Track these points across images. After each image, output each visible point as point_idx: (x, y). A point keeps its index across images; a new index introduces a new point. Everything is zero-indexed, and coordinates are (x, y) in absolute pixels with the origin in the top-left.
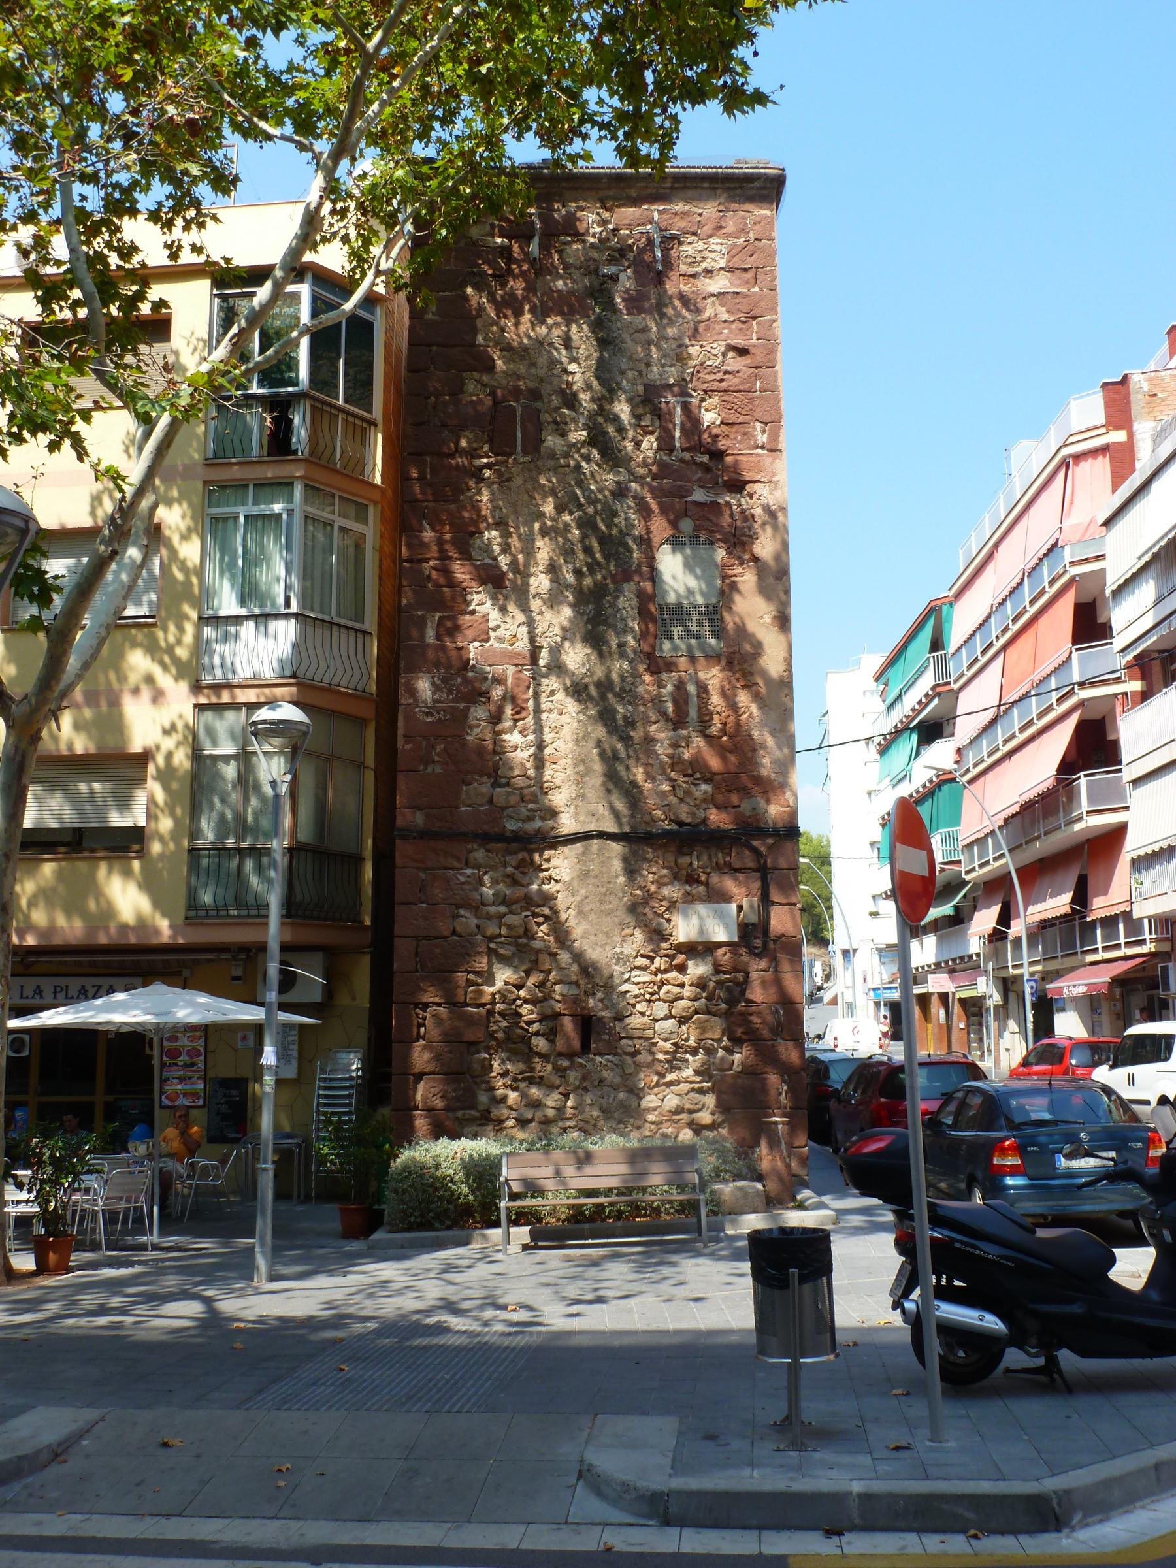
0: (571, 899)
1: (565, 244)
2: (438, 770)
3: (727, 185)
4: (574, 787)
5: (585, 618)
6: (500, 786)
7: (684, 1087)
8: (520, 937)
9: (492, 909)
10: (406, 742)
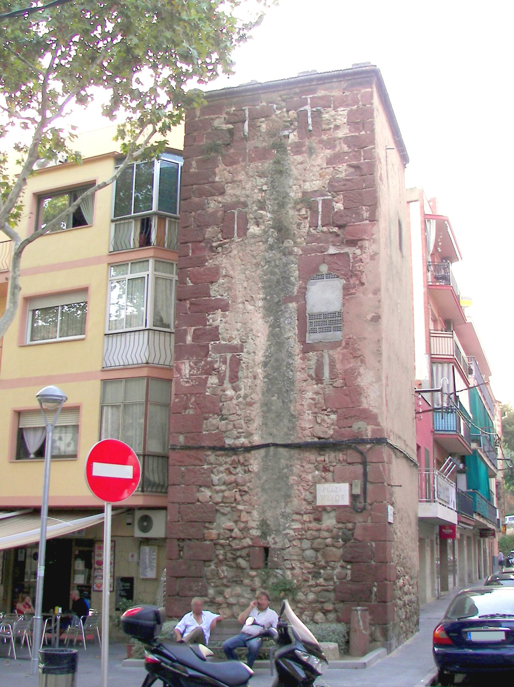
0: (258, 482)
1: (261, 122)
2: (191, 412)
3: (346, 78)
4: (261, 419)
5: (269, 324)
6: (223, 420)
7: (319, 588)
8: (232, 503)
9: (218, 488)
10: (176, 398)
